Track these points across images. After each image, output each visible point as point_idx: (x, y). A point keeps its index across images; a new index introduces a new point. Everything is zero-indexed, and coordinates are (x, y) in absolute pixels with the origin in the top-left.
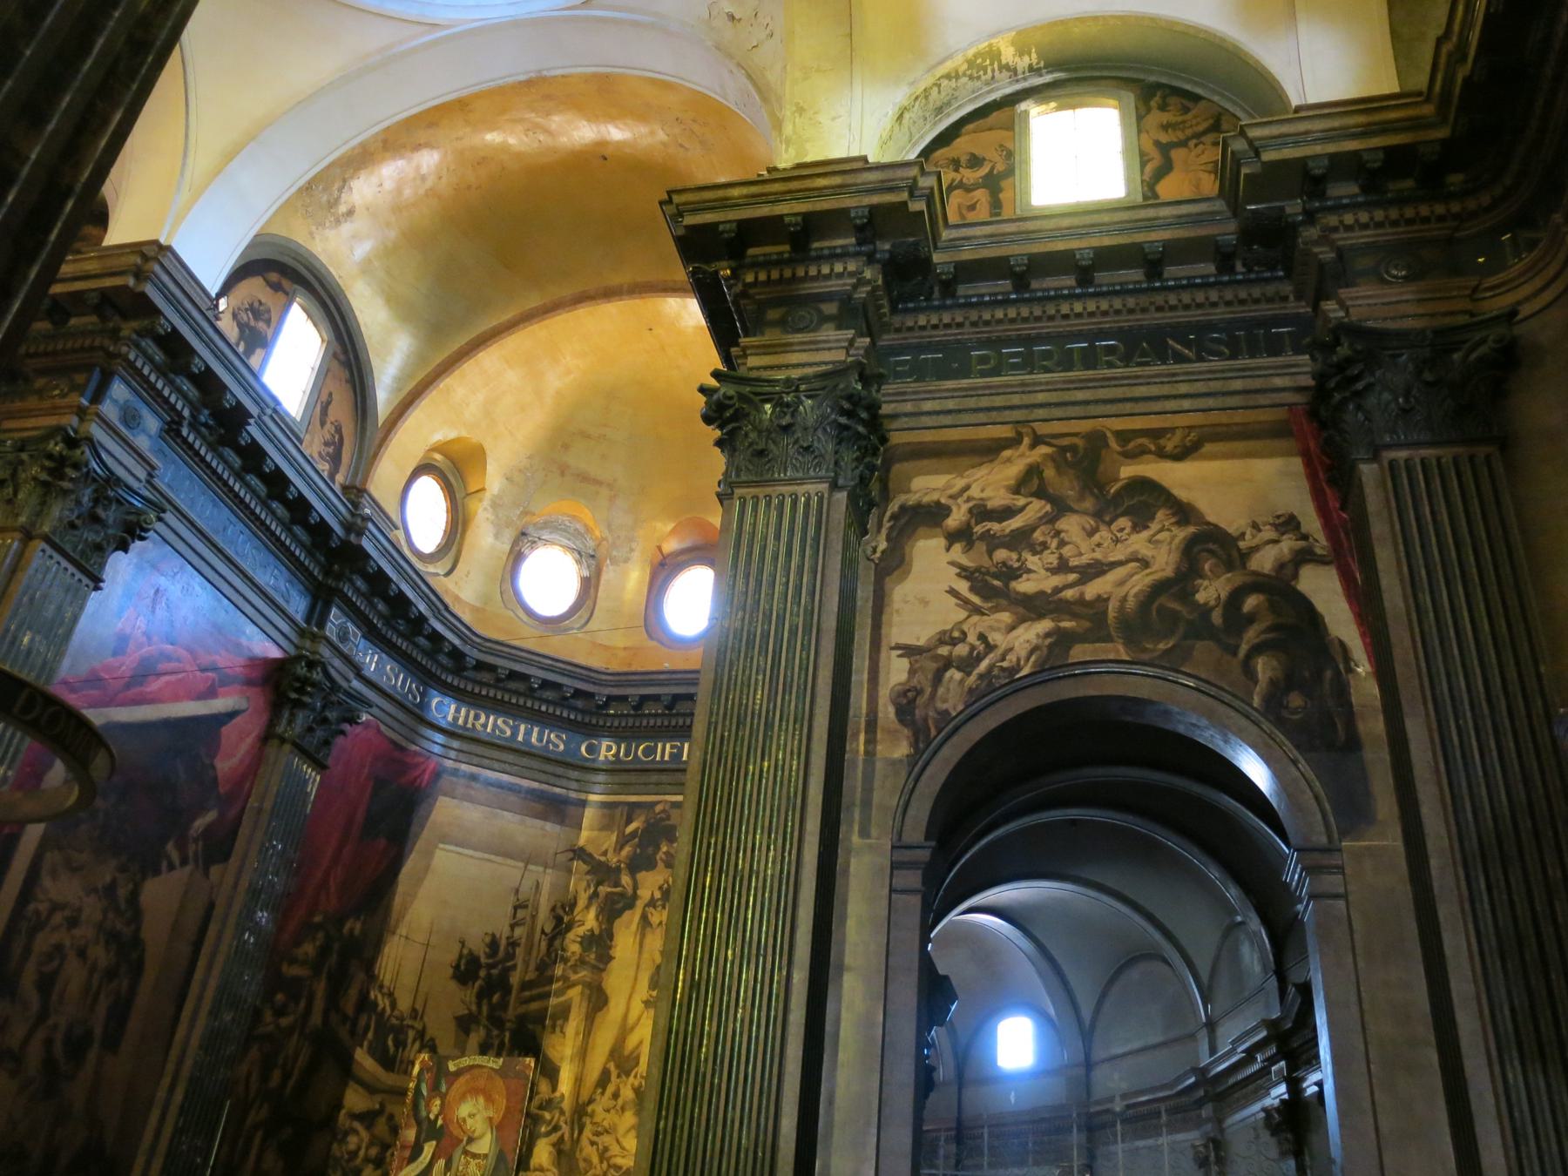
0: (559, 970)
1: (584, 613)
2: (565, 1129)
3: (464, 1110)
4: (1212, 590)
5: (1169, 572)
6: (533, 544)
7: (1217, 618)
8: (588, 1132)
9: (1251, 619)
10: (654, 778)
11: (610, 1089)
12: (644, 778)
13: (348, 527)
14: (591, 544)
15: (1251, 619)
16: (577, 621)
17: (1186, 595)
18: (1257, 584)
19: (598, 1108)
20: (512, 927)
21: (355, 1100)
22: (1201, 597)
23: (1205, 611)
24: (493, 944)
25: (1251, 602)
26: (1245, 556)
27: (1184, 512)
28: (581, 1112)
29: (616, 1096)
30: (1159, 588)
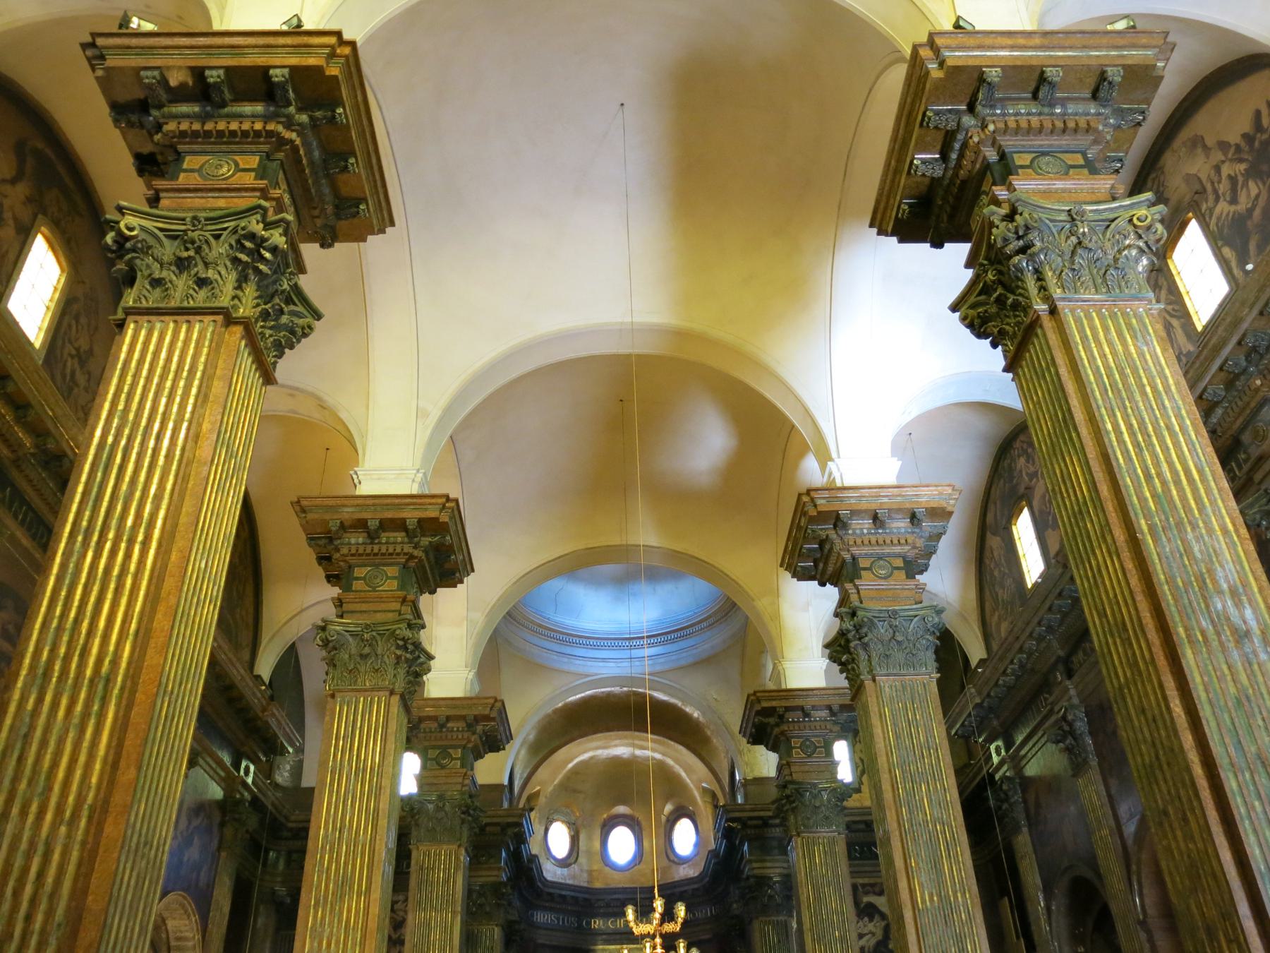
1: (575, 854)
5: (880, 938)
6: (551, 822)
10: (618, 937)
13: (528, 861)
14: (573, 818)
16: (572, 859)
17: (886, 946)
30: (878, 944)
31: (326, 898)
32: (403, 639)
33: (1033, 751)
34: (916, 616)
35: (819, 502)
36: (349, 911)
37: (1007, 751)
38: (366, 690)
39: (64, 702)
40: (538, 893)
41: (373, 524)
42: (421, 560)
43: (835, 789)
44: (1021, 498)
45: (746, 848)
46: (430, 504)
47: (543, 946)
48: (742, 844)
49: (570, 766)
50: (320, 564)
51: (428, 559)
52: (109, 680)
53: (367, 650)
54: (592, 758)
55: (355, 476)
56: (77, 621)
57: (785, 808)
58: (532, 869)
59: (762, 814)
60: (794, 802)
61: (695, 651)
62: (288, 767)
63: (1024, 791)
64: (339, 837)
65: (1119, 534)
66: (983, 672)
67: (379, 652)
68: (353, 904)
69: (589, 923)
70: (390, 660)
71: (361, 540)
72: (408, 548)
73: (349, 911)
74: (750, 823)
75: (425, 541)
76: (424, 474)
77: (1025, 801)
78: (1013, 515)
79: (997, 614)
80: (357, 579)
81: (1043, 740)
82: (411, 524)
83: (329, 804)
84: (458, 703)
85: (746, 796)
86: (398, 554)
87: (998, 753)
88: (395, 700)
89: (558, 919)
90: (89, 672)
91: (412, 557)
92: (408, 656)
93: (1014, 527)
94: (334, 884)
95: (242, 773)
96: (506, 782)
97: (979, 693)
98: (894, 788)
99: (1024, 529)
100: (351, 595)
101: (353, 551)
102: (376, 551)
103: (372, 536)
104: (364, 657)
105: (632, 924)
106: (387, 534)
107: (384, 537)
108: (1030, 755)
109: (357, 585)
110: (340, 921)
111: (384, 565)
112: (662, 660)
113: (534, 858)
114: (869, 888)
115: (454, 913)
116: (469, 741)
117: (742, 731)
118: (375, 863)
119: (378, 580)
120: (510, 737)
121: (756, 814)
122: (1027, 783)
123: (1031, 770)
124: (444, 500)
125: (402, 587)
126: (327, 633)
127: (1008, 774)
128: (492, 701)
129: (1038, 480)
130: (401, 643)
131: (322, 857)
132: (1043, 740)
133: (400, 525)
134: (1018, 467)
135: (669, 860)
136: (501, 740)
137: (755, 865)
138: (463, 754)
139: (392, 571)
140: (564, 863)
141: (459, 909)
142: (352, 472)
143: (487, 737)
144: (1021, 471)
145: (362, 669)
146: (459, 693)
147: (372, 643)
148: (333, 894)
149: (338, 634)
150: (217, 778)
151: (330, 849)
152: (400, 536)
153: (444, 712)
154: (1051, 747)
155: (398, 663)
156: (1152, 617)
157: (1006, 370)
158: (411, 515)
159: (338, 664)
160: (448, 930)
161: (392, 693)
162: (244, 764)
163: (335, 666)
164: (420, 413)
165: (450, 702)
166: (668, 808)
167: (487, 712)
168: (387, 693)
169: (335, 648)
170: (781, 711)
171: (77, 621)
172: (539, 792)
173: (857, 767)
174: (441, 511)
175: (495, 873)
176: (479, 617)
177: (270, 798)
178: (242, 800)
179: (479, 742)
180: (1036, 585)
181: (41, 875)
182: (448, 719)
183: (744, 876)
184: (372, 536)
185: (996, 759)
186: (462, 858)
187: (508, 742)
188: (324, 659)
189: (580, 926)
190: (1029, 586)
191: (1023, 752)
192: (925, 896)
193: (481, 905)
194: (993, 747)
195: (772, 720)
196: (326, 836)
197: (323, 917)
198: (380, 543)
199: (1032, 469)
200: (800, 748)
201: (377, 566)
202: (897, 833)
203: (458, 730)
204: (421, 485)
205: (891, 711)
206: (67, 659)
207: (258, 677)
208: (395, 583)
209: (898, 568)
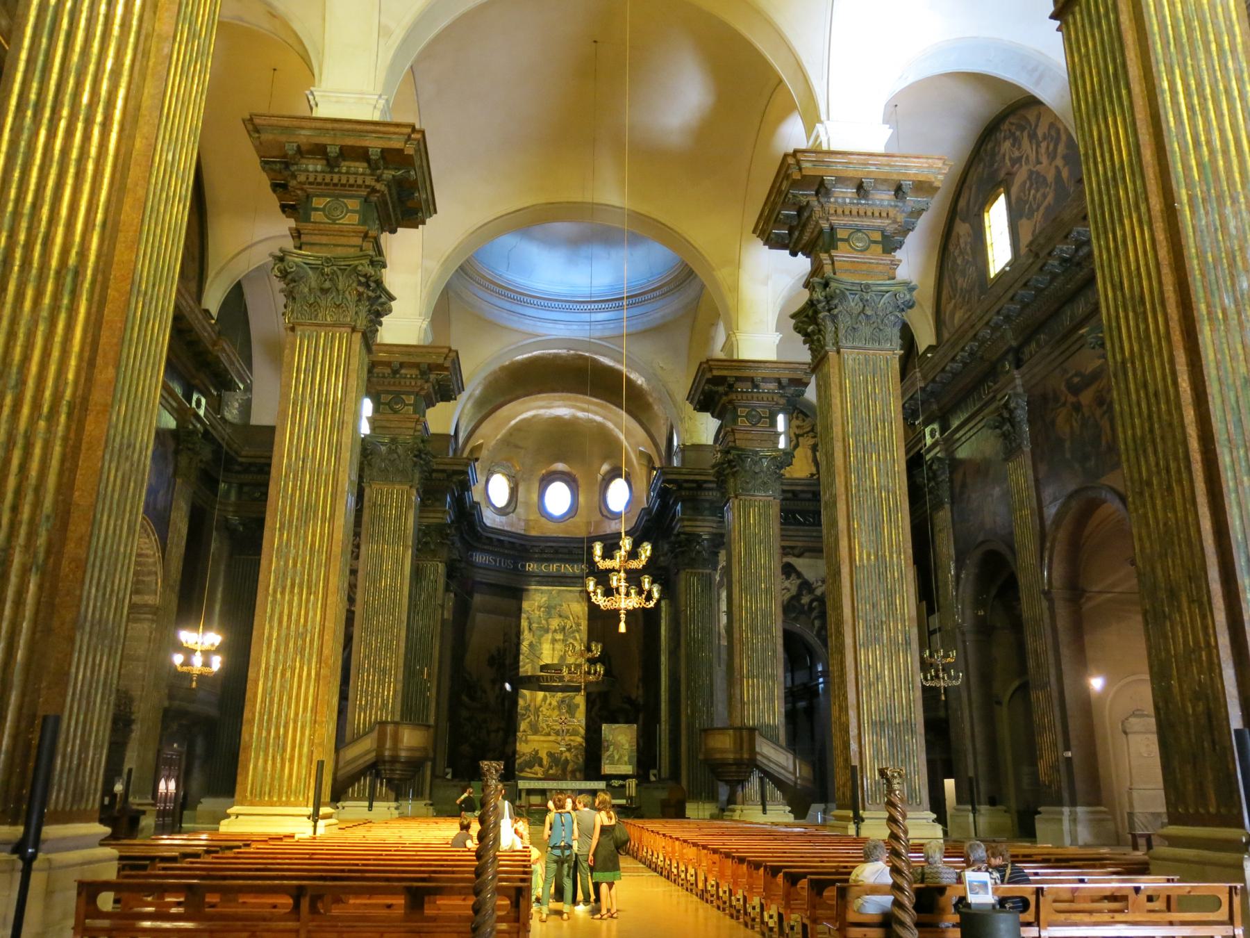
0: (521, 657)
1: (513, 504)
2: (532, 717)
3: (619, 738)
4: (805, 600)
7: (806, 607)
8: (541, 718)
9: (814, 609)
10: (550, 579)
11: (548, 702)
12: (546, 579)
15: (814, 609)
16: (510, 509)
18: (817, 599)
19: (543, 709)
20: (504, 642)
21: (465, 713)
22: (803, 601)
23: (803, 606)
24: (499, 650)
25: (815, 604)
26: (814, 590)
27: (799, 575)
28: (537, 710)
29: (550, 704)
30: (793, 598)
31: (291, 522)
32: (365, 276)
33: (968, 435)
34: (887, 292)
35: (804, 165)
36: (314, 535)
37: (942, 434)
38: (327, 325)
39: (30, 293)
40: (478, 537)
41: (333, 151)
42: (383, 195)
43: (775, 458)
44: (999, 184)
45: (679, 507)
46: (395, 133)
47: (482, 583)
48: (675, 503)
49: (513, 422)
50: (274, 191)
51: (390, 194)
52: (78, 273)
53: (327, 285)
54: (534, 417)
55: (311, 97)
56: (36, 206)
57: (726, 472)
58: (474, 515)
59: (698, 478)
60: (735, 466)
61: (645, 319)
62: (236, 405)
63: (951, 473)
64: (303, 467)
65: (1156, 203)
66: (932, 357)
67: (340, 287)
68: (316, 531)
69: (523, 566)
70: (351, 297)
71: (319, 168)
72: (370, 181)
73: (314, 535)
74: (686, 485)
75: (388, 174)
76: (387, 101)
77: (951, 481)
78: (986, 201)
79: (953, 301)
80: (316, 209)
81: (980, 426)
82: (374, 154)
83: (292, 434)
84: (412, 350)
85: (683, 460)
86: (359, 186)
87: (932, 435)
88: (357, 337)
89: (495, 561)
90: (54, 263)
91: (374, 190)
92: (370, 294)
93: (986, 215)
94: (299, 510)
95: (194, 405)
96: (452, 433)
97: (924, 377)
98: (846, 455)
99: (997, 218)
100: (310, 226)
101: (311, 179)
102: (335, 181)
103: (332, 164)
104: (325, 291)
105: (597, 559)
106: (347, 163)
107: (345, 166)
108: (963, 439)
109: (315, 216)
110: (305, 544)
111: (345, 197)
112: (612, 326)
113: (476, 505)
114: (788, 550)
115: (405, 547)
116: (422, 389)
117: (690, 398)
118: (339, 493)
119: (339, 213)
120: (461, 389)
121: (692, 477)
122: (955, 464)
123: (962, 453)
124: (409, 130)
125: (364, 221)
126: (285, 264)
127: (939, 455)
128: (446, 351)
129: (1021, 165)
130: (363, 280)
131: (286, 484)
132: (980, 426)
133: (362, 154)
134: (1002, 151)
135: (603, 515)
136: (453, 391)
137: (686, 523)
138: (415, 400)
139: (354, 204)
140: (502, 512)
141: (410, 543)
142: (307, 92)
143: (439, 385)
144: (1004, 155)
145: (323, 304)
146: (414, 342)
147: (332, 278)
148: (297, 519)
149: (297, 266)
150: (169, 408)
151: (294, 478)
152: (361, 167)
153: (398, 358)
154: (987, 432)
155: (359, 300)
156: (1175, 291)
157: (1053, 17)
158: (375, 145)
159: (297, 296)
160: (398, 562)
161: (354, 330)
162: (195, 397)
163: (294, 299)
164: (383, 31)
165: (405, 349)
166: (605, 468)
167: (440, 361)
168: (349, 330)
169: (293, 281)
170: (731, 380)
171: (36, 206)
172: (482, 444)
173: (791, 441)
174: (406, 143)
175: (440, 515)
176: (435, 266)
177: (222, 434)
178: (195, 431)
179: (431, 390)
180: (1003, 273)
181: (23, 467)
182: (402, 365)
183: (675, 532)
184: (332, 164)
185: (929, 441)
186: (413, 498)
187: (460, 393)
188: (282, 291)
189: (516, 568)
190: (992, 275)
191: (957, 436)
192: (863, 555)
193: (426, 543)
194: (928, 430)
195: (721, 389)
196: (289, 465)
197: (289, 540)
198: (340, 172)
199: (1017, 154)
200: (745, 417)
201: (337, 197)
202: (844, 497)
203: (411, 378)
204: (383, 112)
205: (852, 383)
206: (28, 247)
207: (207, 311)
208: (356, 217)
209: (875, 242)
